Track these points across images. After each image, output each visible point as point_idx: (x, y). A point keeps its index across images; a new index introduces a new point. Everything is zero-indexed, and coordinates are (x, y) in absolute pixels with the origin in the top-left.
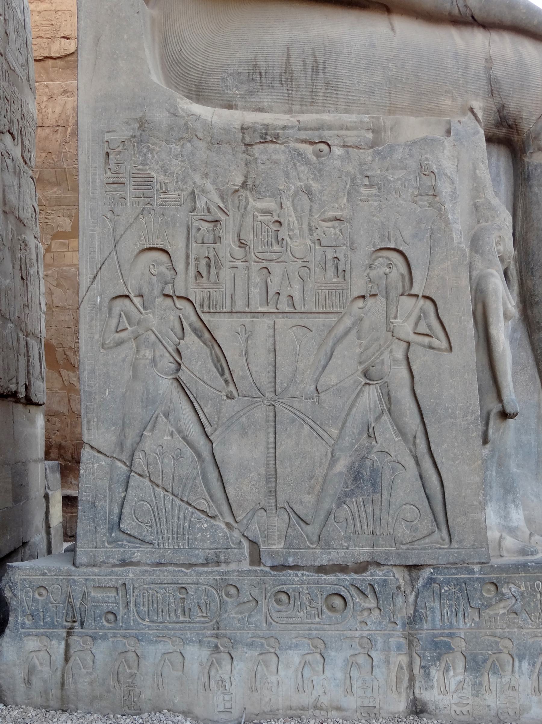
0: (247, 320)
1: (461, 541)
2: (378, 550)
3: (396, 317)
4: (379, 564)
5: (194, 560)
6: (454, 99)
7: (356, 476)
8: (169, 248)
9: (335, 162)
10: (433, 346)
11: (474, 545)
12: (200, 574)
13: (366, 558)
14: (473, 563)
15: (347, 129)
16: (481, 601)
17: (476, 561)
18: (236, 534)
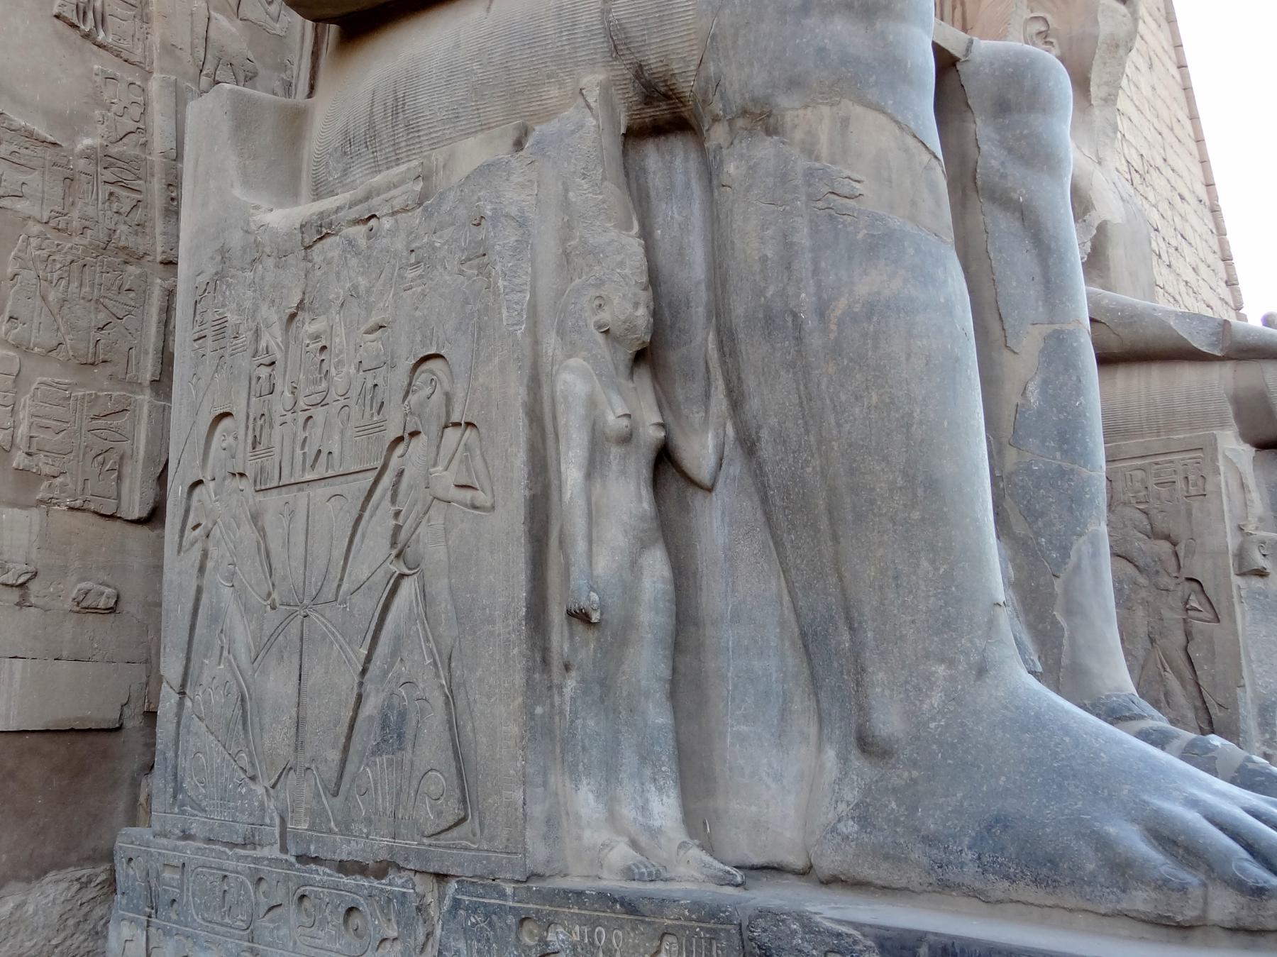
1: (491, 839)
2: (400, 842)
3: (435, 465)
6: (561, 84)
9: (384, 241)
10: (477, 504)
11: (507, 847)
13: (383, 855)
14: (505, 880)
15: (395, 187)
16: (517, 949)
17: (508, 876)
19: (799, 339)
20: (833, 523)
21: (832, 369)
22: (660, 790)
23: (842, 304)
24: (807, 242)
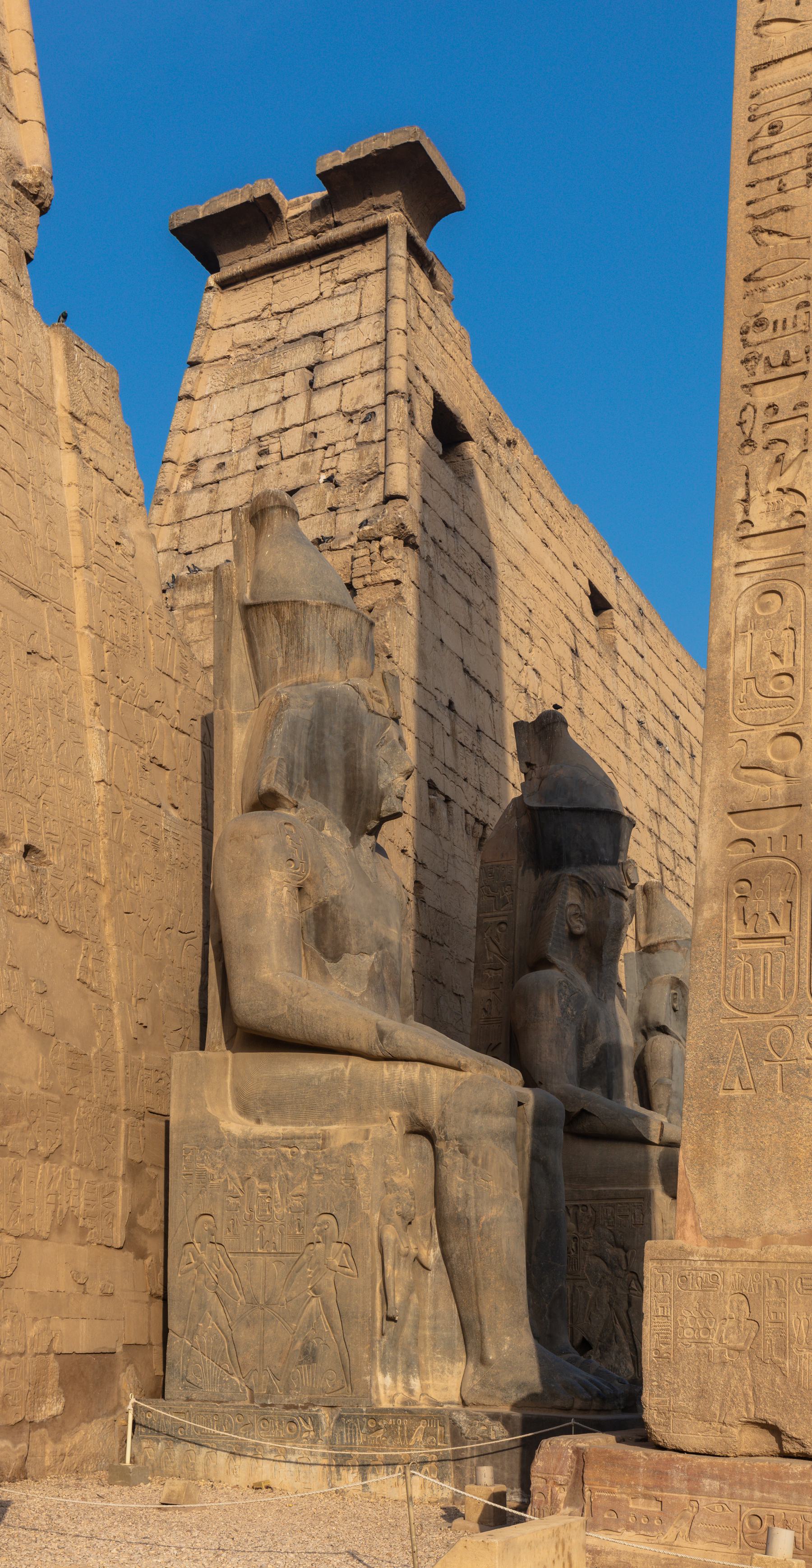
0: (252, 1257)
1: (356, 1393)
4: (314, 1406)
5: (222, 1399)
7: (305, 1353)
8: (213, 1214)
12: (225, 1407)
18: (243, 1385)
19: (469, 1228)
20: (476, 1289)
21: (479, 1239)
22: (414, 1377)
23: (484, 1219)
24: (473, 1195)
